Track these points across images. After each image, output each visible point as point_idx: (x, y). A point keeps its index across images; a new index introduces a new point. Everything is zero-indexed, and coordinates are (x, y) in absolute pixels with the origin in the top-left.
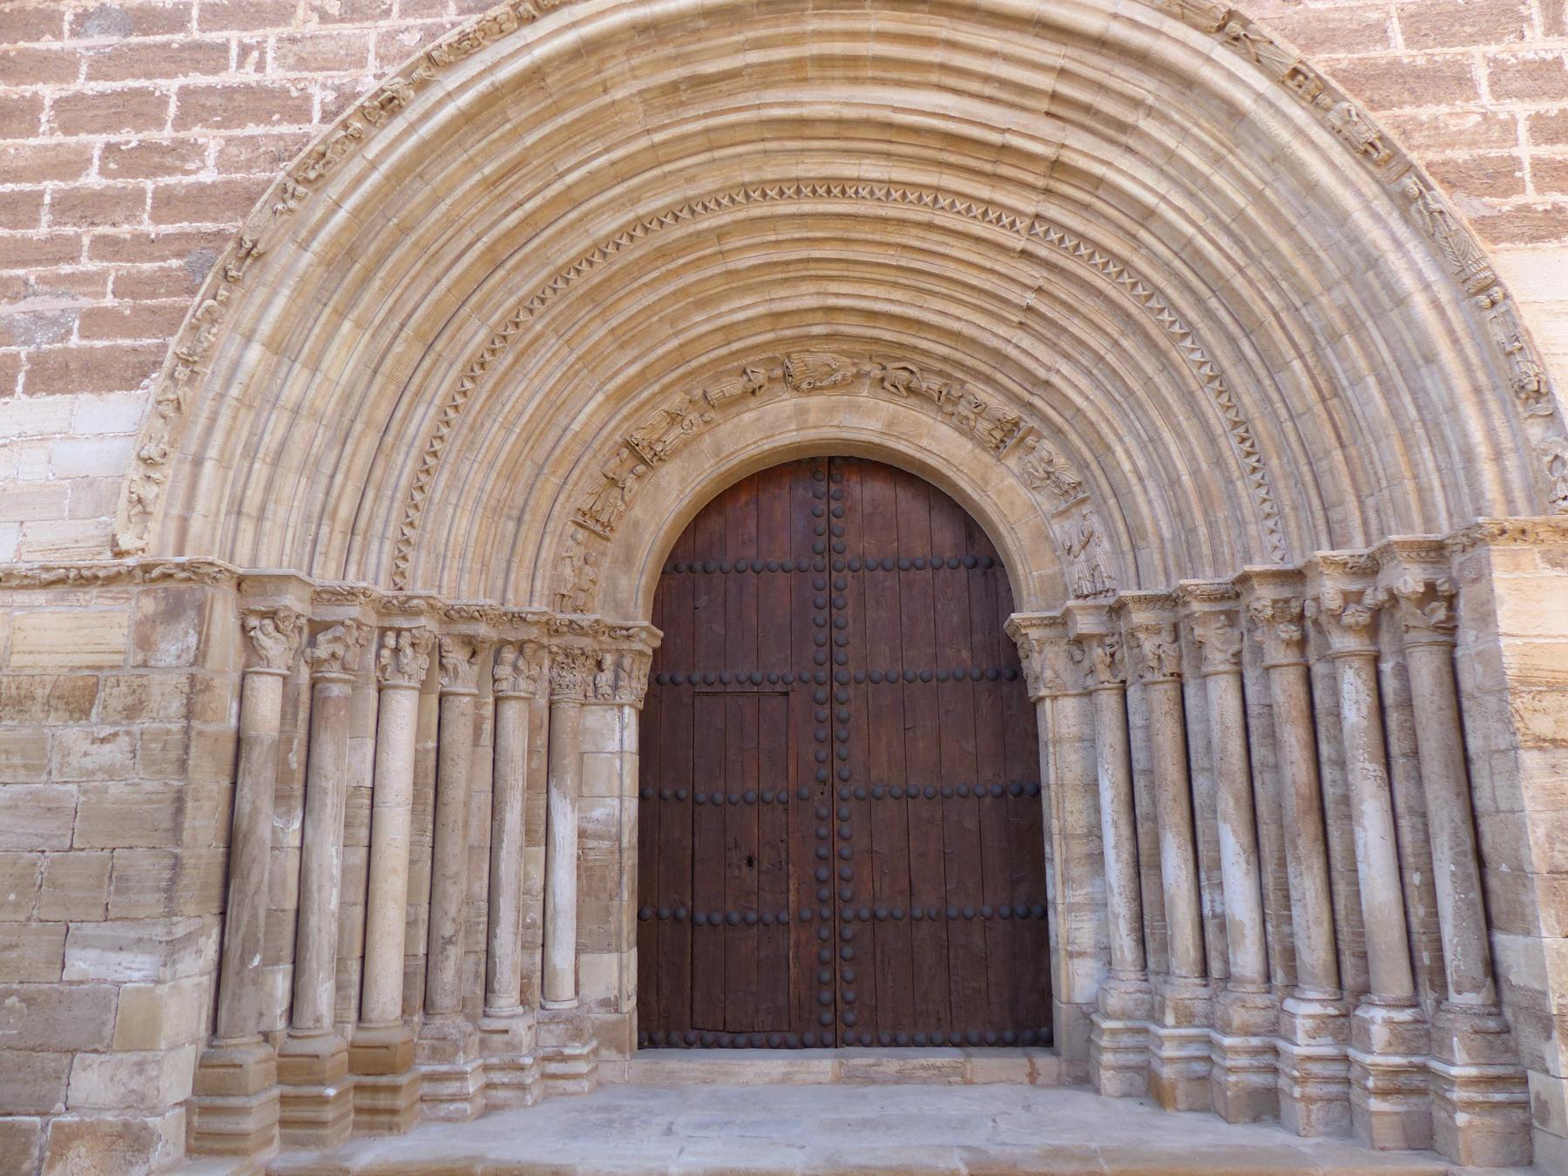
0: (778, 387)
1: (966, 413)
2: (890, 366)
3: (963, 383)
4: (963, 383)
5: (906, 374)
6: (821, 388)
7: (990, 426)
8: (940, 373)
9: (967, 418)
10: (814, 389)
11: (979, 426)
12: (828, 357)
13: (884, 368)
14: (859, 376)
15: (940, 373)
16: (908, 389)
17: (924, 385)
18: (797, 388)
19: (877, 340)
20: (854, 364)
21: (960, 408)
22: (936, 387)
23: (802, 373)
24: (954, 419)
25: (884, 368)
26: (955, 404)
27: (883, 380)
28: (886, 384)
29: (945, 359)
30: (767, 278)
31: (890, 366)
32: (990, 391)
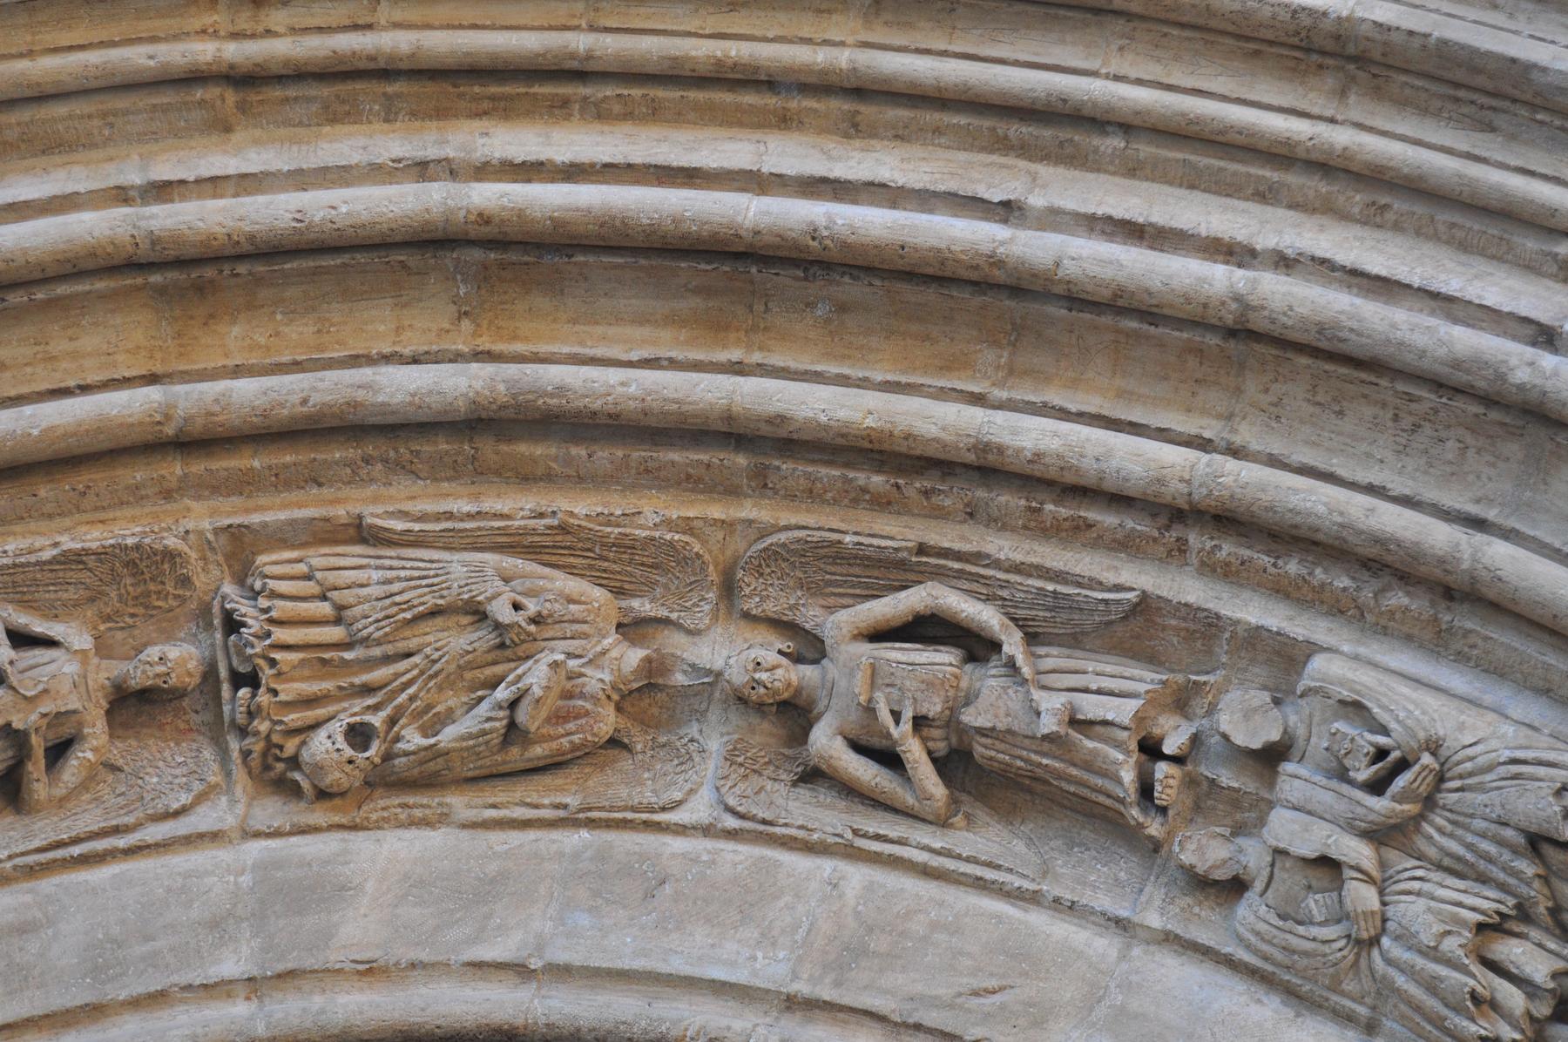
0: (171, 766)
1: (1312, 838)
2: (838, 623)
3: (1287, 658)
4: (1287, 658)
5: (944, 658)
6: (428, 777)
7: (1487, 901)
8: (1135, 628)
9: (1328, 865)
10: (397, 781)
11: (1413, 912)
12: (460, 571)
13: (809, 648)
14: (651, 699)
15: (1135, 628)
16: (955, 763)
17: (1051, 705)
18: (279, 774)
19: (768, 444)
20: (632, 628)
21: (1284, 828)
22: (1122, 711)
23: (321, 658)
24: (1251, 911)
25: (809, 648)
26: (1245, 816)
27: (794, 714)
28: (826, 741)
29: (1178, 518)
30: (138, 58)
31: (838, 623)
32: (1457, 680)
